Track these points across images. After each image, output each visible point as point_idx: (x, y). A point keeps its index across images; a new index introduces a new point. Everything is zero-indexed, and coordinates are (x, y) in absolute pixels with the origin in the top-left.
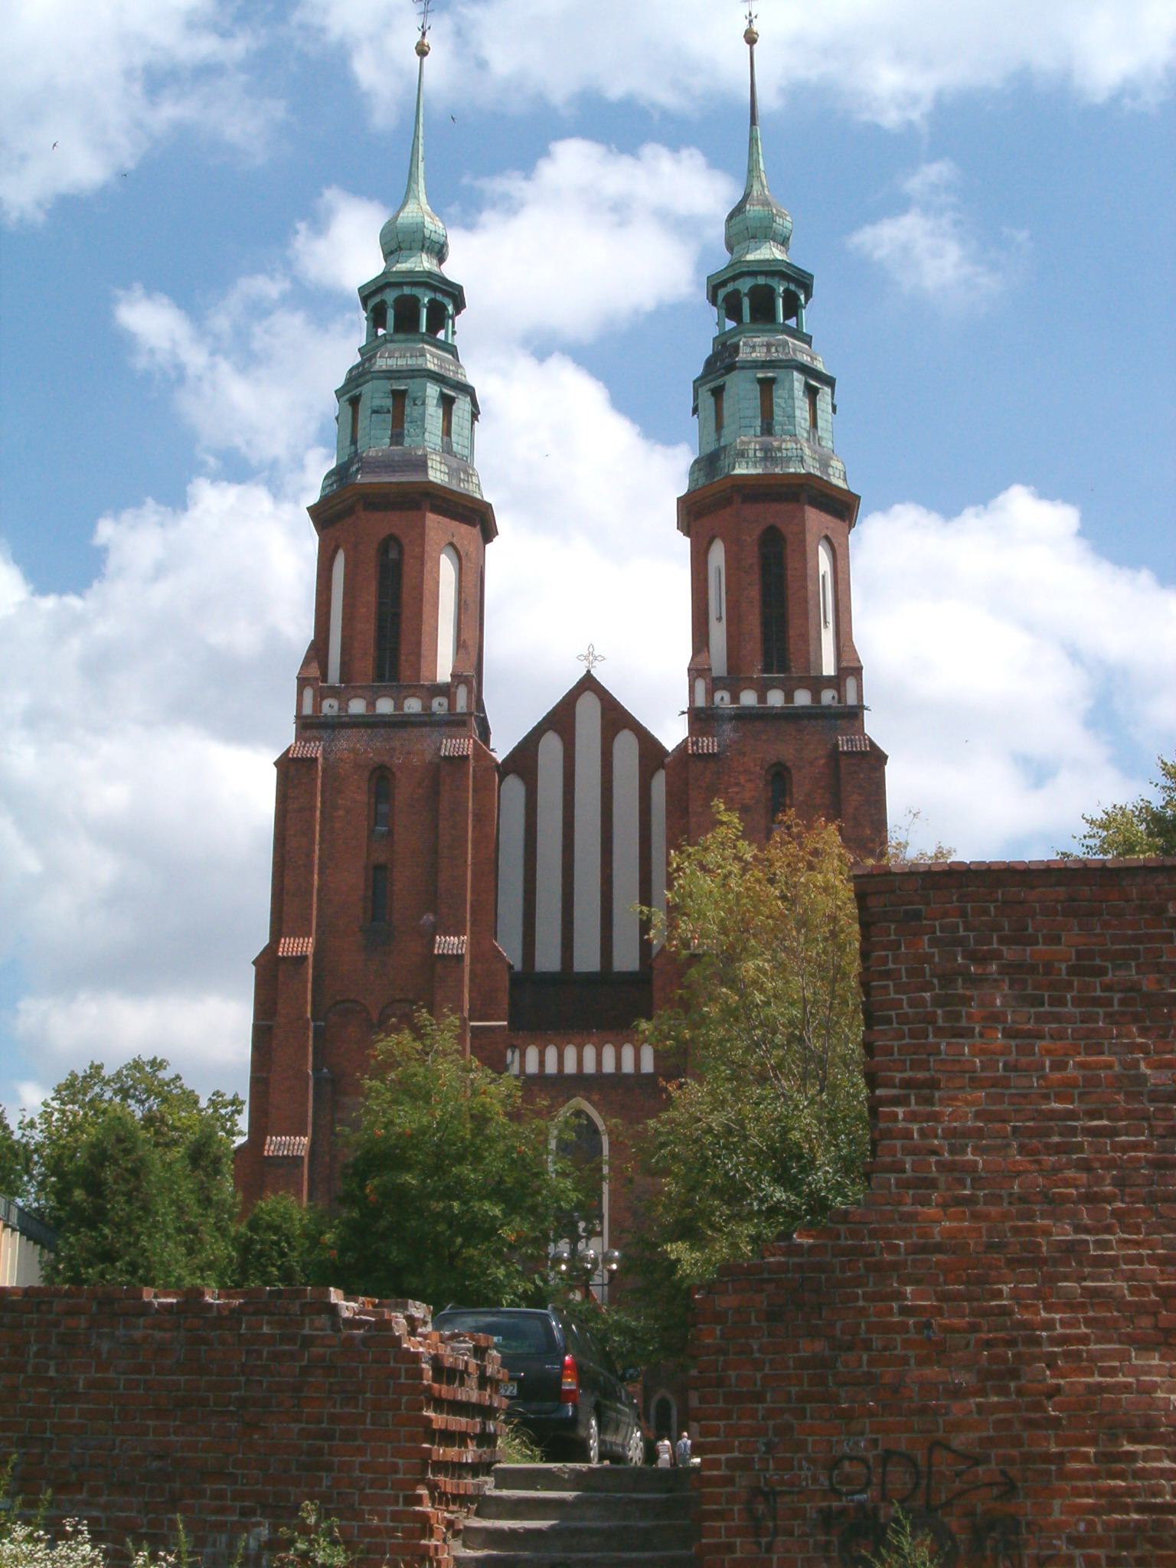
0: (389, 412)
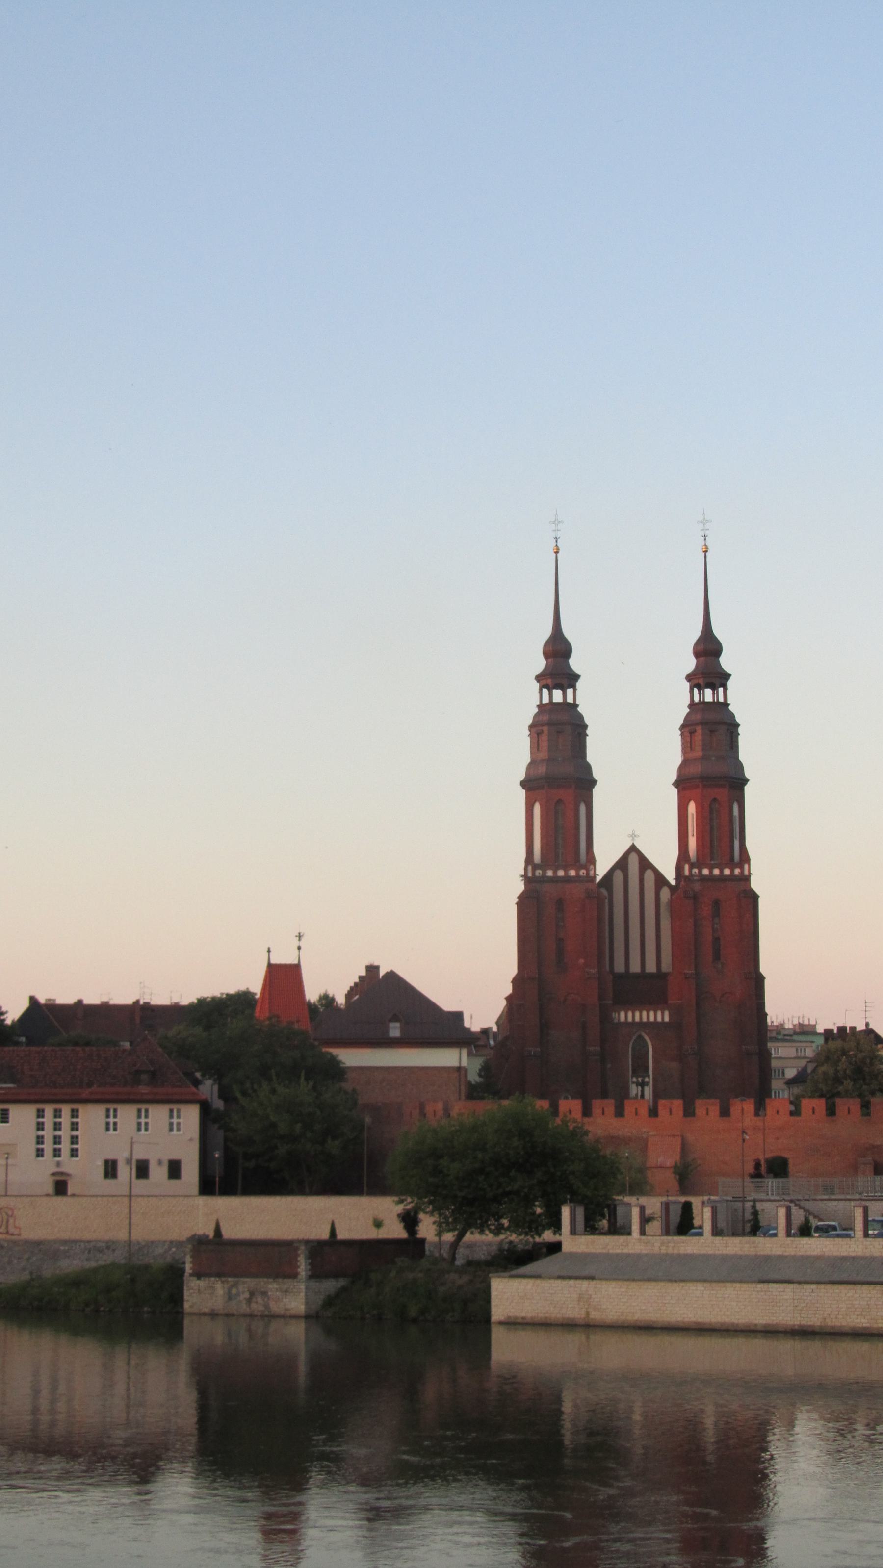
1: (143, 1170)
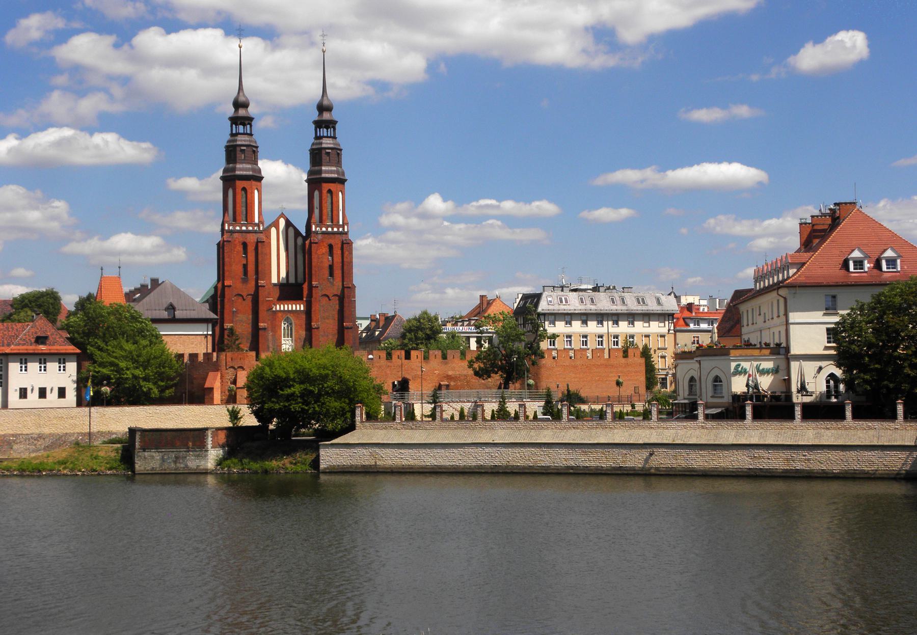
1: (43, 393)
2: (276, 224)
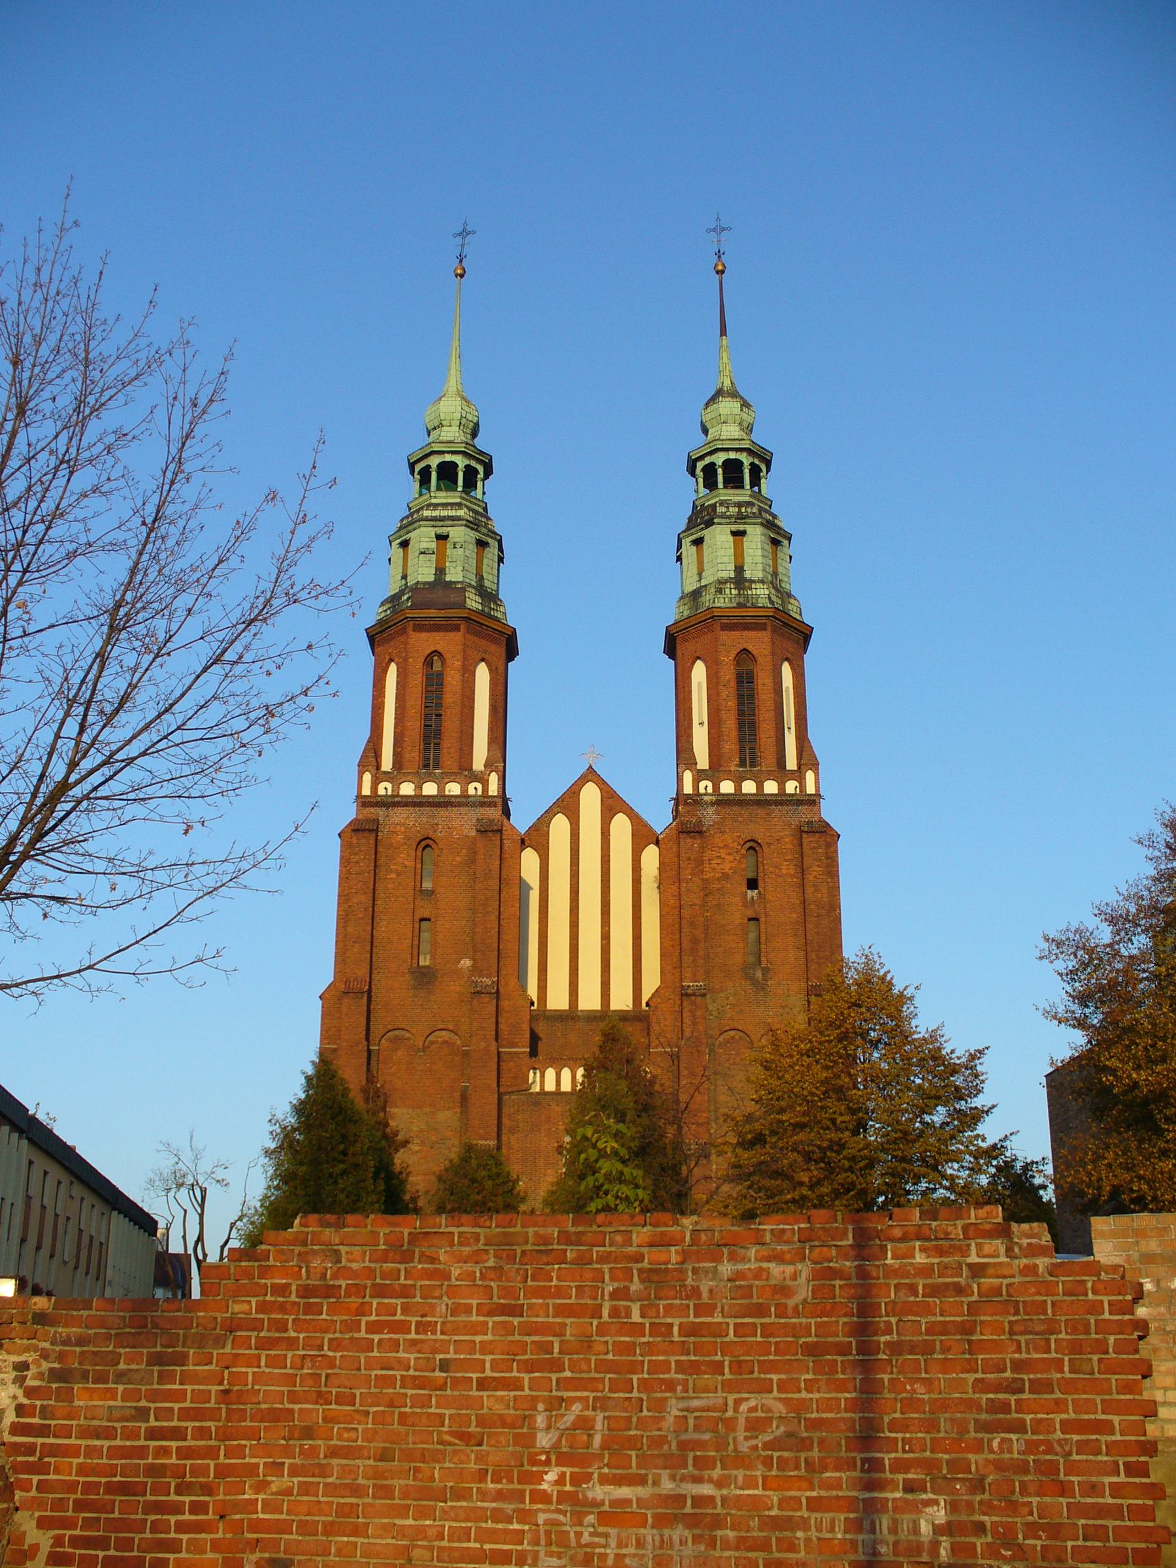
0: (433, 553)
2: (568, 804)
